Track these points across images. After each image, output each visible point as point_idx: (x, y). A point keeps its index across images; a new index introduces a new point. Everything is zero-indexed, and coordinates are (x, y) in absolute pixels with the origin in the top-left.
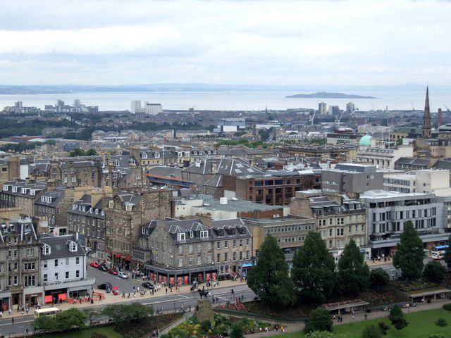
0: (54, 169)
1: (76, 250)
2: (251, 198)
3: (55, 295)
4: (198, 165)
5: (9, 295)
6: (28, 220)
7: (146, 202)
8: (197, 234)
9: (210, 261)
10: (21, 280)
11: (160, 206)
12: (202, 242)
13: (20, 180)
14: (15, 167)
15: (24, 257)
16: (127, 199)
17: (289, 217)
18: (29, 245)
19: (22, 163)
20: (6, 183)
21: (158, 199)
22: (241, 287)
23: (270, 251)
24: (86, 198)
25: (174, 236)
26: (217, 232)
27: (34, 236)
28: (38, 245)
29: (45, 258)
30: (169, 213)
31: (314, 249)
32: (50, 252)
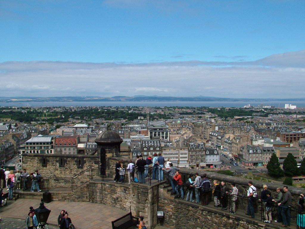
0: (226, 128)
1: (217, 153)
2: (284, 140)
3: (209, 166)
4: (271, 128)
5: (195, 164)
6: (203, 143)
7: (243, 140)
8: (256, 151)
9: (261, 160)
10: (199, 161)
11: (247, 141)
12: (258, 153)
13: (215, 131)
14: (214, 127)
15: (201, 154)
16: (237, 138)
17: (292, 147)
18: (202, 151)
19: (216, 126)
20: (211, 132)
21: (247, 139)
22: (265, 168)
23: (274, 158)
24: (229, 138)
25: (249, 151)
26: (265, 151)
27: (203, 149)
28: (204, 151)
29: (206, 155)
30: (251, 143)
31: (290, 159)
32: (208, 153)
